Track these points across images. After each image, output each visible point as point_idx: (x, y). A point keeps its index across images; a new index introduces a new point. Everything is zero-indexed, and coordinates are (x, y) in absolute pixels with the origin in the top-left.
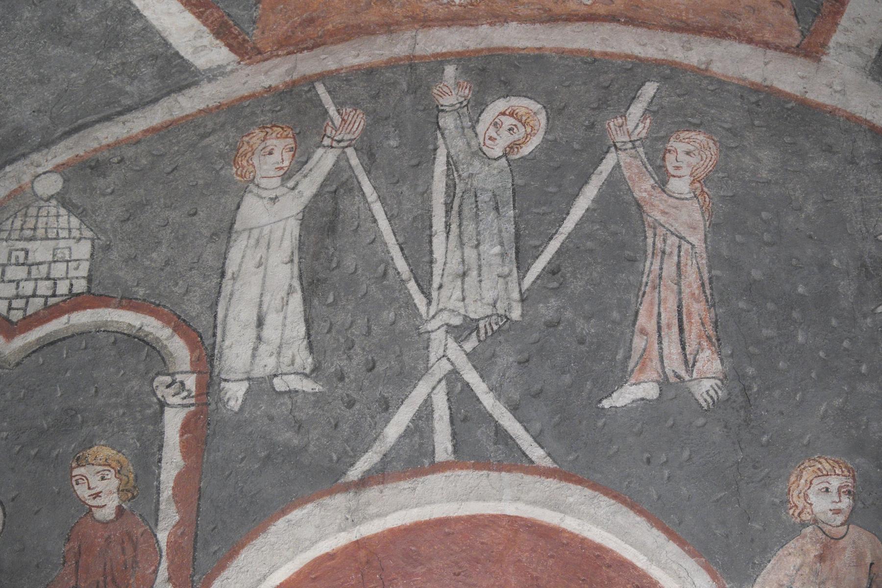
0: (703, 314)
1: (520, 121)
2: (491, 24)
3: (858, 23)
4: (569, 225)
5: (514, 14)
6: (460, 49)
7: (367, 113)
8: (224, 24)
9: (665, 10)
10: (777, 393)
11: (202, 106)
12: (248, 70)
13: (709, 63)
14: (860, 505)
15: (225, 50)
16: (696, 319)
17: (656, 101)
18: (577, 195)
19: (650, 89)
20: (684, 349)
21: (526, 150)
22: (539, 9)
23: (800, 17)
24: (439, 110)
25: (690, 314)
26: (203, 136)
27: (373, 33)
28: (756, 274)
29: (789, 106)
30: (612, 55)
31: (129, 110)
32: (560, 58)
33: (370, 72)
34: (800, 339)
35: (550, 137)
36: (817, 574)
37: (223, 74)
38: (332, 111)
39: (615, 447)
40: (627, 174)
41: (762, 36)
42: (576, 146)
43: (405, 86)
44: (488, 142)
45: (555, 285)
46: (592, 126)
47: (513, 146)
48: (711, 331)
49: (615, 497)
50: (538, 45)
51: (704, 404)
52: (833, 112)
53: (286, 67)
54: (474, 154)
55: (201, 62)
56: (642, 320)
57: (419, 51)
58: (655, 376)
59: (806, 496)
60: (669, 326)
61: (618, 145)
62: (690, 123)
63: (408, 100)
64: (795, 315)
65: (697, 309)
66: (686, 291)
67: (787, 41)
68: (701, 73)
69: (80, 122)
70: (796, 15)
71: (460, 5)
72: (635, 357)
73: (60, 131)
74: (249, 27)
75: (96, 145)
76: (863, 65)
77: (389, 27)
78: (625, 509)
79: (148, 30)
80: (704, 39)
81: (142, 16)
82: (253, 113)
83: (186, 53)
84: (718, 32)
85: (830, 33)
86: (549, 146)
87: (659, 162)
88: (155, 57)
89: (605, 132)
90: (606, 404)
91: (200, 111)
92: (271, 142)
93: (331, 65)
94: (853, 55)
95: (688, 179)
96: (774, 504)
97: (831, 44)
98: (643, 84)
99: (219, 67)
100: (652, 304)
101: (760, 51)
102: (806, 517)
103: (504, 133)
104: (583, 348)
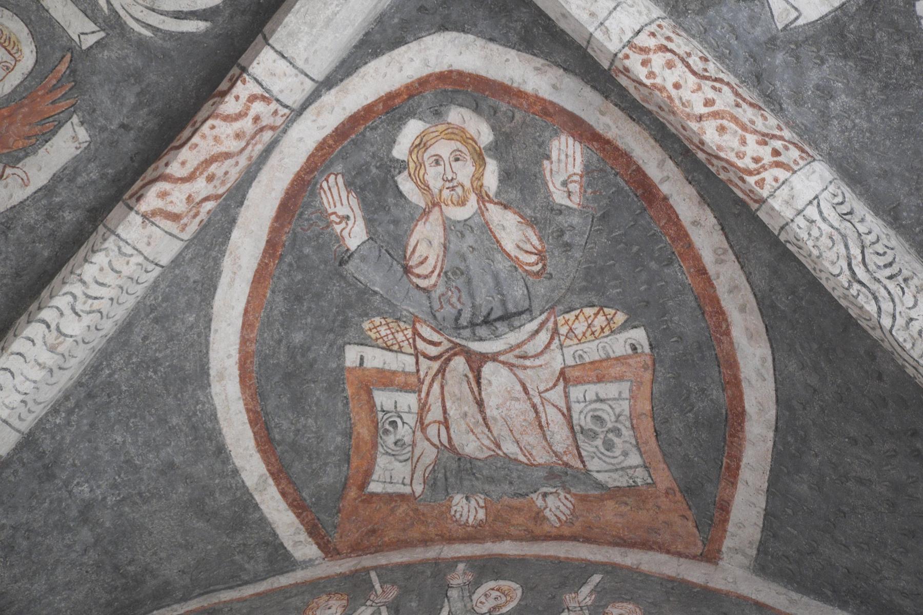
1: (503, 593)
2: (493, 542)
3: (740, 527)
5: (507, 533)
6: (470, 555)
7: (400, 587)
8: (315, 526)
9: (608, 529)
11: (293, 582)
12: (330, 563)
15: (315, 547)
17: (600, 585)
19: (597, 578)
21: (504, 610)
22: (525, 530)
23: (700, 528)
24: (449, 587)
26: (287, 598)
27: (416, 546)
29: (695, 590)
30: (572, 559)
32: (537, 560)
33: (407, 566)
35: (522, 603)
37: (312, 566)
38: (377, 586)
41: (676, 548)
42: (540, 608)
43: (429, 573)
44: (479, 604)
46: (554, 597)
52: (727, 594)
53: (353, 563)
57: (443, 555)
61: (570, 608)
62: (623, 598)
63: (429, 581)
68: (634, 572)
69: (212, 588)
70: (697, 527)
71: (473, 526)
73: (197, 591)
74: (332, 531)
75: (217, 601)
76: (748, 564)
77: (426, 542)
79: (263, 521)
80: (636, 550)
81: (259, 509)
82: (325, 587)
83: (288, 545)
84: (645, 545)
85: (722, 538)
88: (267, 543)
91: (291, 585)
92: (331, 602)
94: (739, 558)
97: (724, 549)
98: (592, 575)
99: (311, 560)
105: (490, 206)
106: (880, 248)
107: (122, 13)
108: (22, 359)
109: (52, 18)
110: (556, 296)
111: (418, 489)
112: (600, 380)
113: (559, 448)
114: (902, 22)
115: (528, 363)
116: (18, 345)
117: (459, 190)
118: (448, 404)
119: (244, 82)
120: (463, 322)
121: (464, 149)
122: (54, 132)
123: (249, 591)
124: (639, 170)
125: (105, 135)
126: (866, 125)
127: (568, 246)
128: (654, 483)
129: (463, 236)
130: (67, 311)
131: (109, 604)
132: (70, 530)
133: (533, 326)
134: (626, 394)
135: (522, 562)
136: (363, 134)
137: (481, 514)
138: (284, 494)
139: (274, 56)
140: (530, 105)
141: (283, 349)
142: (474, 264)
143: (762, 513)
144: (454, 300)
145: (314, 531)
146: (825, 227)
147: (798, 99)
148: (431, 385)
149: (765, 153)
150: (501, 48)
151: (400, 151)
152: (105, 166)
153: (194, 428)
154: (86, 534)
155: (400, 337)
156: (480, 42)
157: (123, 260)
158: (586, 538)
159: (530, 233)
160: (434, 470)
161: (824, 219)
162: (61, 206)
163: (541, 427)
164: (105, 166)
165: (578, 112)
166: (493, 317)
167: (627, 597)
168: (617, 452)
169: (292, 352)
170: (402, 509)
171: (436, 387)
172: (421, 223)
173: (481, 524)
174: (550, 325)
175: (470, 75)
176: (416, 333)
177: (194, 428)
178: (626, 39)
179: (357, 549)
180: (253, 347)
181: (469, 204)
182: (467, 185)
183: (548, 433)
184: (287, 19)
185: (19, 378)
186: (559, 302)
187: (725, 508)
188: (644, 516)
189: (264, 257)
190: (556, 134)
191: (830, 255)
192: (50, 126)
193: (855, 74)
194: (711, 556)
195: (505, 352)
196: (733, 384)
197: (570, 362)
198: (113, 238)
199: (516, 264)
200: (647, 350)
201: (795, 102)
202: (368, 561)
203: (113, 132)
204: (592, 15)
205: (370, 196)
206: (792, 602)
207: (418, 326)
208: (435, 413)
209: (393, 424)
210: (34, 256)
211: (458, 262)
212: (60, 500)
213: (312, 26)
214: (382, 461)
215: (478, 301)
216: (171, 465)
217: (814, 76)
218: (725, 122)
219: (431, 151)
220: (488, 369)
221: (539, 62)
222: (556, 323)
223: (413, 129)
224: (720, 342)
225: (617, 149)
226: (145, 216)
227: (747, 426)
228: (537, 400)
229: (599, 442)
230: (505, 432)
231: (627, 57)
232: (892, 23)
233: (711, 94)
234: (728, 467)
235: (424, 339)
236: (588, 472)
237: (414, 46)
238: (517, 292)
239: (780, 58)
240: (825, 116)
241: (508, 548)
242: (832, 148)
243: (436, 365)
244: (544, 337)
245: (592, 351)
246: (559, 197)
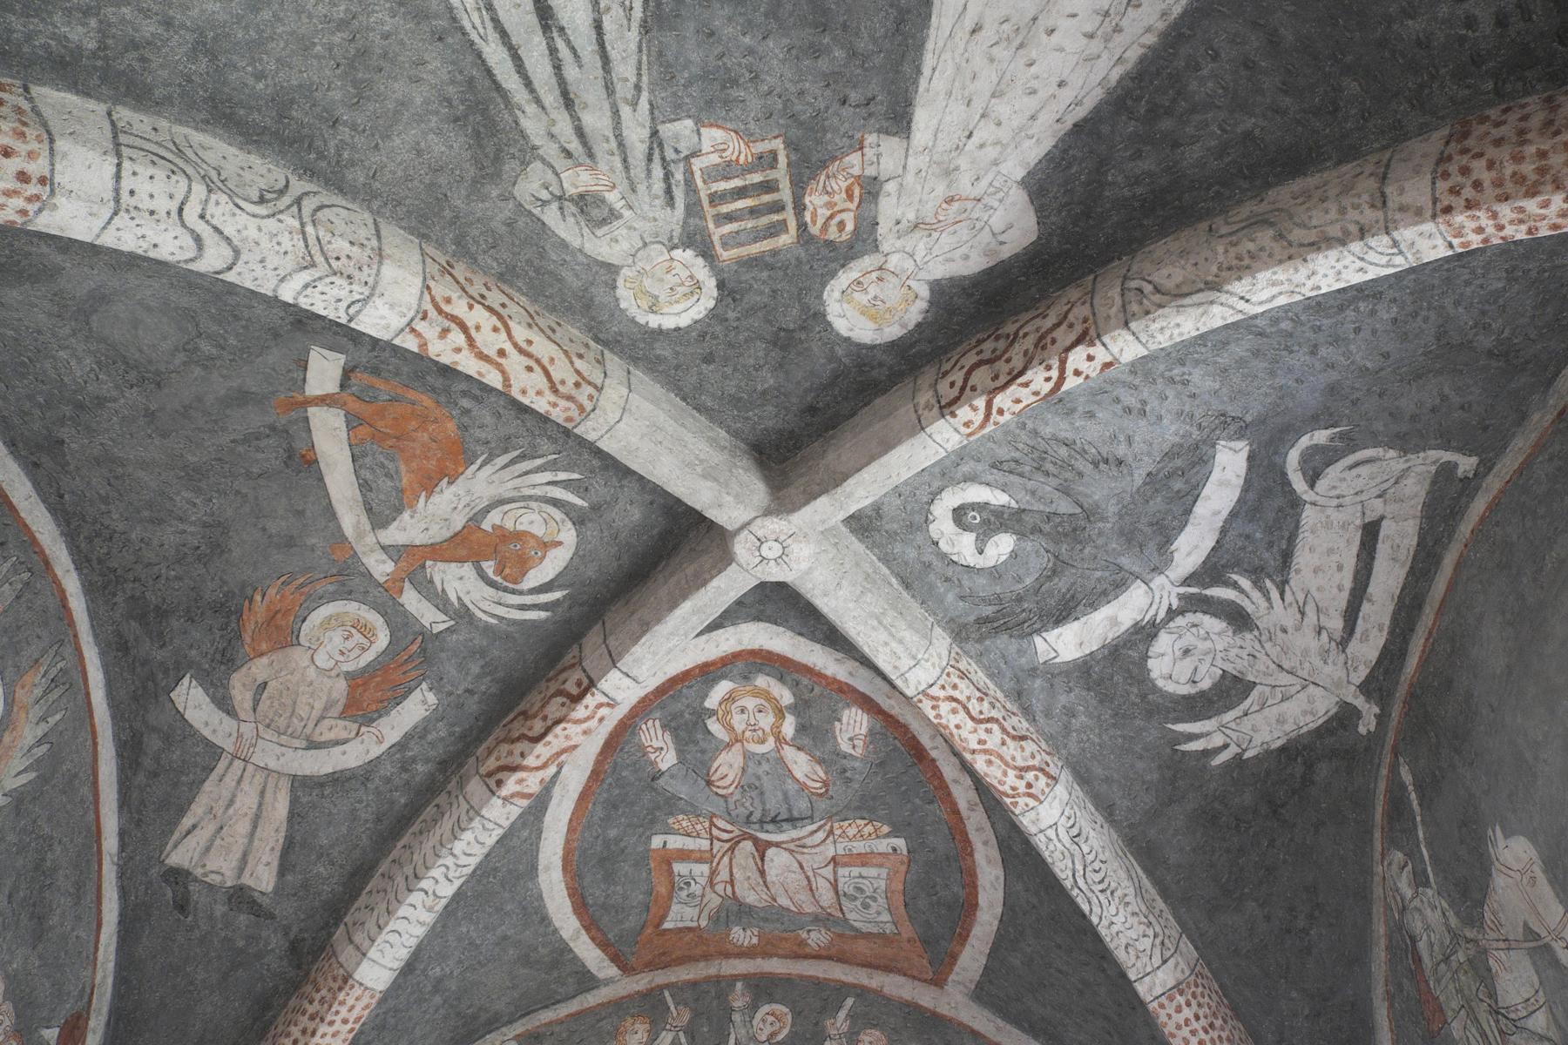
8: (617, 955)
13: (882, 987)
15: (615, 969)
19: (850, 1002)
21: (780, 1037)
26: (598, 1021)
31: (558, 1002)
33: (694, 984)
38: (672, 1008)
46: (817, 1024)
47: (773, 1035)
52: (950, 1020)
54: (751, 1039)
55: (601, 975)
63: (715, 1003)
67: (925, 976)
68: (878, 993)
77: (706, 957)
79: (576, 958)
83: (594, 970)
84: (888, 969)
86: (793, 1035)
89: (824, 1027)
92: (637, 1026)
93: (673, 979)
97: (950, 979)
103: (768, 1026)
105: (785, 747)
106: (1097, 865)
107: (471, 606)
108: (406, 922)
109: (406, 611)
110: (834, 811)
111: (703, 923)
112: (863, 865)
113: (825, 904)
114: (1135, 671)
115: (805, 850)
116: (403, 911)
117: (760, 733)
118: (735, 871)
119: (593, 695)
120: (757, 816)
121: (766, 704)
122: (405, 696)
123: (564, 1010)
124: (914, 737)
125: (452, 698)
126: (1097, 740)
127: (850, 780)
128: (900, 934)
129: (760, 763)
130: (442, 879)
131: (452, 1039)
132: (426, 1000)
133: (814, 827)
134: (884, 876)
135: (788, 980)
136: (680, 691)
137: (755, 940)
138: (593, 939)
139: (621, 675)
140: (828, 684)
141: (600, 842)
142: (767, 783)
144: (747, 804)
145: (616, 959)
146: (1059, 845)
147: (1048, 714)
148: (722, 858)
149: (1021, 785)
150: (808, 642)
151: (712, 702)
152: (452, 725)
153: (524, 908)
154: (438, 999)
155: (699, 827)
156: (789, 634)
157: (487, 834)
158: (841, 958)
159: (818, 768)
160: (718, 911)
161: (1060, 841)
162: (414, 760)
163: (811, 890)
164: (452, 725)
165: (868, 693)
166: (779, 818)
168: (872, 911)
169: (607, 843)
170: (688, 937)
171: (726, 859)
172: (724, 753)
173: (754, 946)
174: (827, 827)
175: (778, 655)
176: (712, 824)
177: (524, 908)
178: (921, 689)
179: (651, 966)
180: (576, 844)
181: (767, 744)
182: (768, 729)
183: (817, 894)
184: (633, 649)
185: (405, 937)
186: (836, 814)
187: (954, 958)
189: (588, 781)
190: (848, 706)
191: (1061, 865)
192: (401, 690)
193: (1094, 702)
194: (938, 981)
195: (787, 842)
196: (971, 885)
197: (840, 852)
198: (478, 819)
199: (803, 787)
200: (905, 852)
201: (1046, 716)
202: (661, 977)
203: (459, 696)
204: (895, 667)
205: (682, 734)
206: (998, 1029)
207: (715, 820)
208: (724, 875)
209: (688, 884)
210: (392, 803)
211: (753, 780)
212: (419, 983)
213: (655, 654)
214: (675, 908)
215: (768, 807)
216: (505, 938)
217: (1063, 699)
218: (993, 758)
219: (738, 703)
220: (771, 852)
221: (840, 655)
222: (832, 827)
223: (723, 687)
224: (964, 859)
225: (898, 722)
226: (505, 799)
227: (978, 914)
228: (810, 874)
229: (858, 903)
230: (781, 891)
231: (920, 701)
232: (1128, 671)
233: (984, 736)
234: (960, 934)
235: (719, 829)
236: (846, 920)
237: (731, 629)
238: (802, 805)
239: (1038, 682)
240: (1067, 728)
241: (776, 966)
242: (1069, 754)
243: (727, 845)
244: (821, 835)
245: (859, 847)
246: (845, 747)
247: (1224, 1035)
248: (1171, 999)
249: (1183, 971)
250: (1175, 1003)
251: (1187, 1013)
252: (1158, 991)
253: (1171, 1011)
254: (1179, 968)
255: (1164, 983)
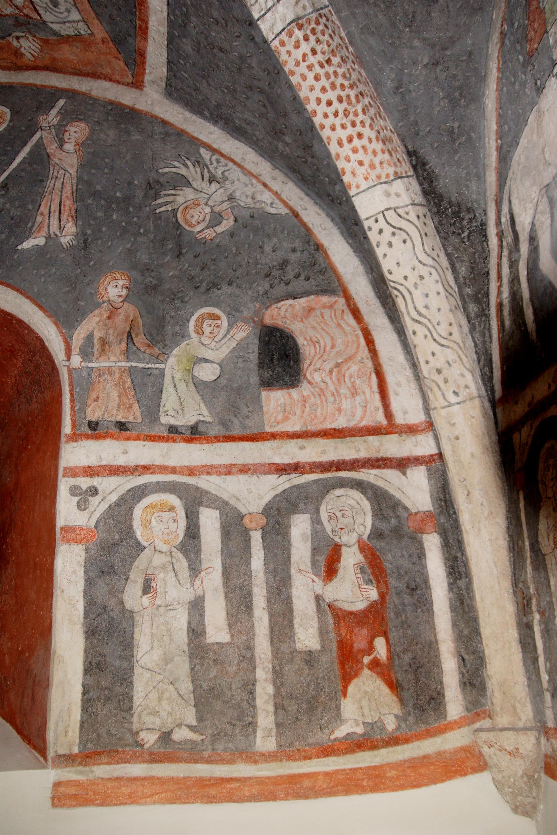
0: (71, 206)
4: (14, 165)
10: (99, 242)
13: (90, 91)
14: (131, 293)
16: (67, 208)
17: (64, 108)
18: (20, 151)
19: (61, 102)
20: (60, 222)
25: (65, 205)
28: (98, 187)
29: (126, 111)
34: (115, 217)
36: (106, 325)
39: (21, 268)
40: (45, 141)
42: (23, 129)
45: (3, 192)
46: (32, 119)
48: (73, 213)
49: (17, 290)
50: (11, 81)
51: (65, 247)
52: (146, 113)
56: (42, 209)
58: (44, 234)
59: (106, 289)
60: (54, 211)
64: (114, 206)
65: (68, 203)
66: (64, 195)
68: (86, 96)
70: (126, 65)
72: (36, 225)
78: (20, 296)
80: (89, 79)
84: (95, 76)
87: (61, 136)
89: (37, 122)
90: (19, 247)
95: (73, 144)
96: (91, 293)
97: (145, 81)
100: (47, 201)
101: (115, 85)
102: (105, 299)
104: (13, 222)
143: (166, 60)
167: (81, 117)
187: (142, 55)
188: (90, 56)
247: (340, 71)
248: (290, 35)
249: (304, 8)
250: (293, 39)
251: (305, 48)
252: (279, 27)
253: (290, 47)
254: (301, 4)
255: (283, 20)
